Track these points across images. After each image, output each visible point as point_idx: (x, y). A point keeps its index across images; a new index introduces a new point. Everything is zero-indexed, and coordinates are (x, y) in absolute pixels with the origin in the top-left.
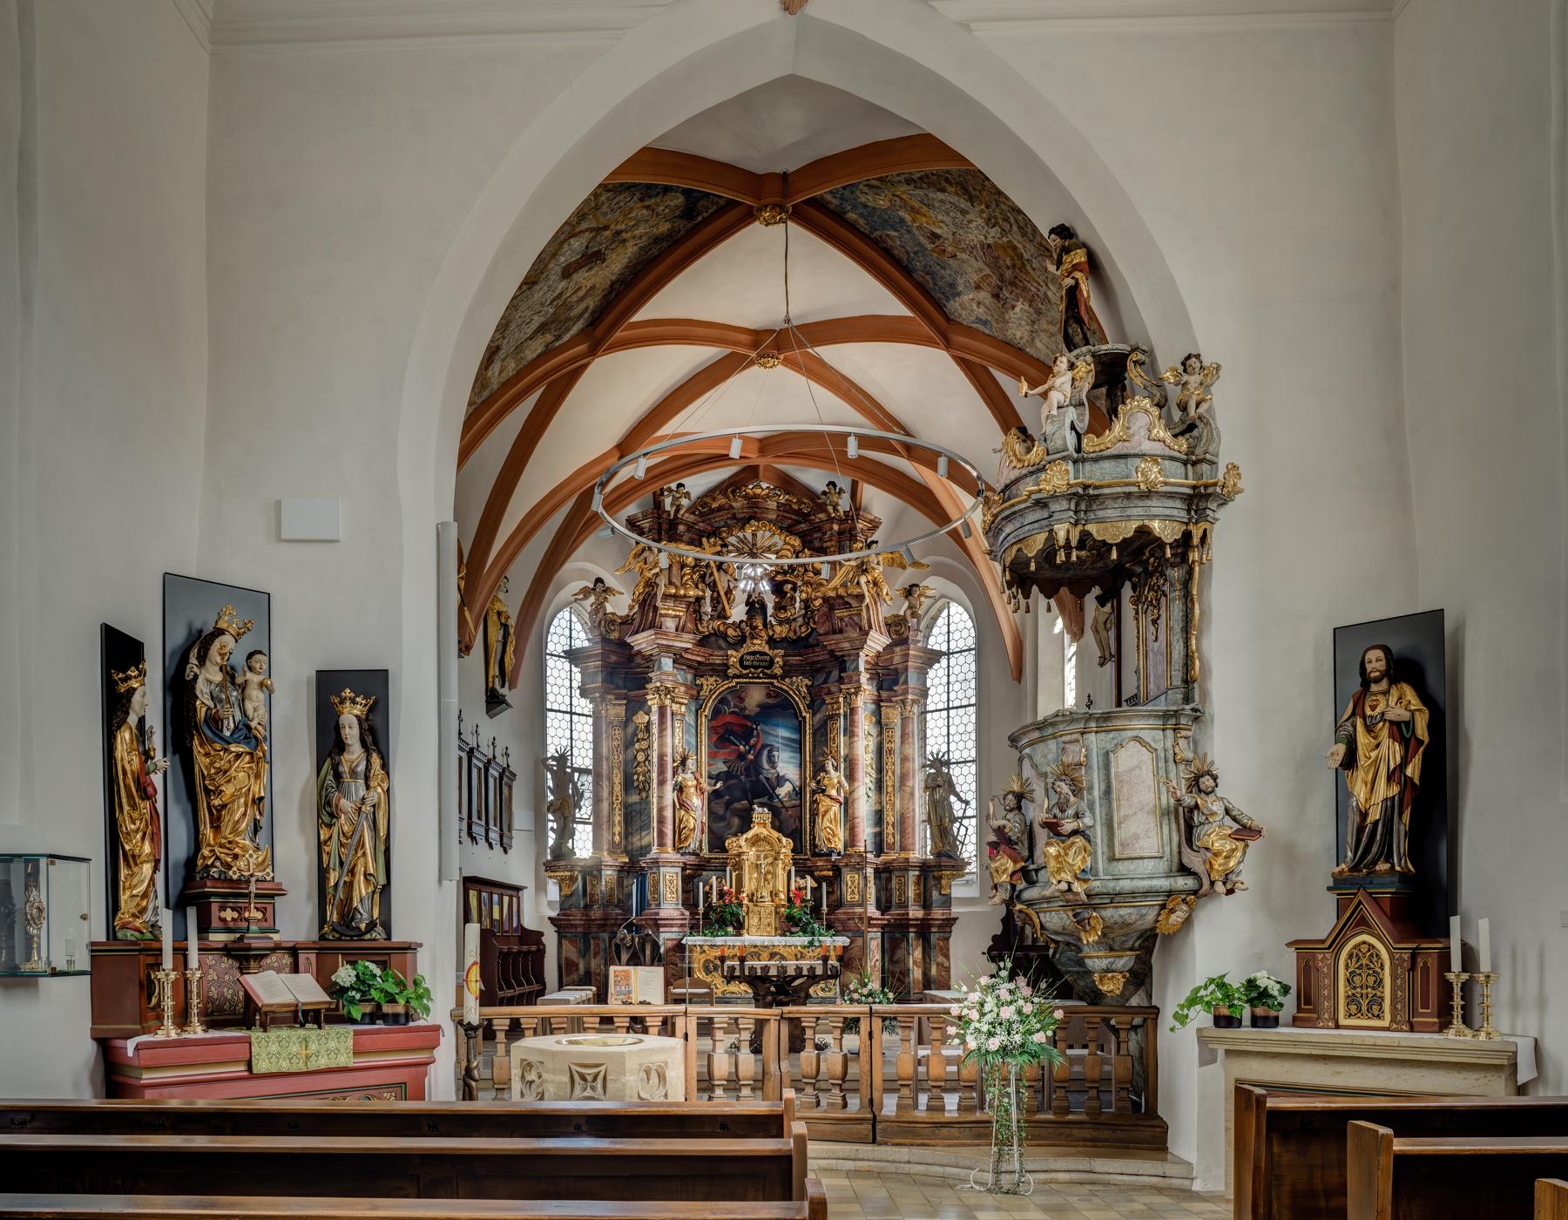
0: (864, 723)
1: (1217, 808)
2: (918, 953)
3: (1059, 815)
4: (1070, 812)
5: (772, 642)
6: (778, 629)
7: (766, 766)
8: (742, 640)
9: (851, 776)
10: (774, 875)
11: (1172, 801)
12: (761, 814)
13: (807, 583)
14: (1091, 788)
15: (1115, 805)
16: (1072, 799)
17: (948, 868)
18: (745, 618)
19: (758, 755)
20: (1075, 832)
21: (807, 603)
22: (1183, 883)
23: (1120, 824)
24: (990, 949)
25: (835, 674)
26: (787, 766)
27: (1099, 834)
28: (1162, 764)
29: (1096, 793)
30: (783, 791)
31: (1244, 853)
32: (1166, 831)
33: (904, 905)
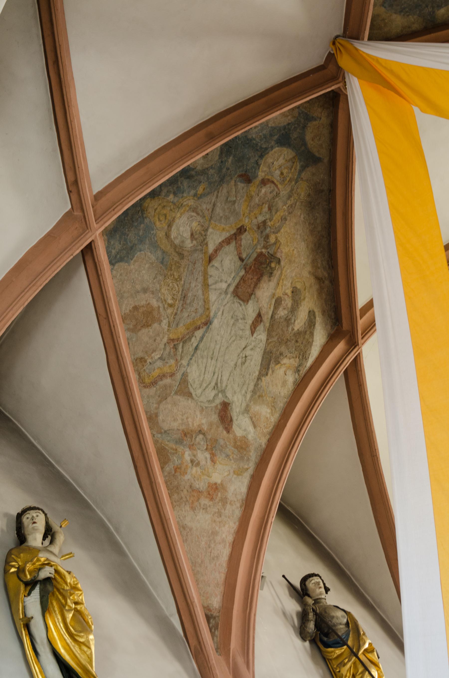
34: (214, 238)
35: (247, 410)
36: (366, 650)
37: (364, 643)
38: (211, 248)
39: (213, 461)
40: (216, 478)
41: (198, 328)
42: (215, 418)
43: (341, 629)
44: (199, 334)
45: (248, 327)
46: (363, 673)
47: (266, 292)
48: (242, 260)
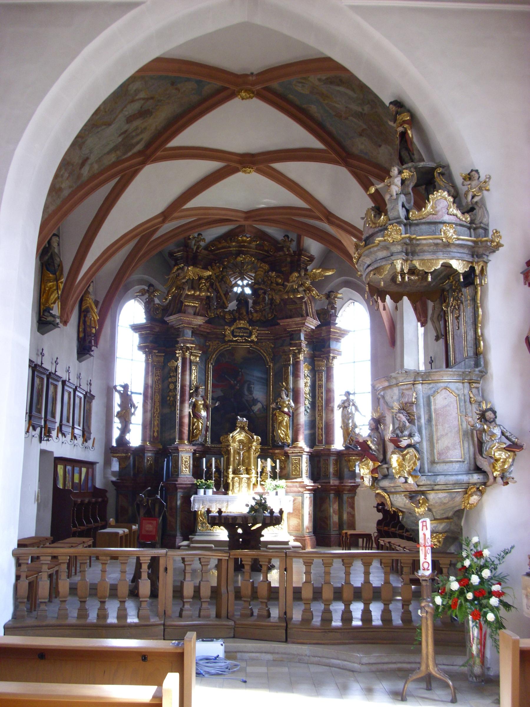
0: (304, 370)
1: (497, 431)
2: (336, 506)
3: (400, 434)
4: (406, 433)
5: (251, 322)
6: (255, 315)
9: (296, 400)
10: (249, 458)
11: (469, 427)
13: (272, 289)
14: (419, 418)
15: (434, 429)
16: (408, 424)
18: (236, 308)
20: (409, 446)
21: (272, 300)
22: (476, 478)
23: (438, 440)
26: (258, 393)
27: (425, 446)
28: (462, 404)
29: (423, 421)
30: (257, 408)
31: (513, 460)
32: (466, 445)
33: (327, 476)
34: (142, 95)
35: (92, 164)
38: (137, 97)
39: (67, 179)
40: (63, 186)
41: (105, 125)
42: (80, 161)
44: (103, 127)
45: (120, 133)
46: (55, 290)
47: (137, 123)
48: (141, 108)
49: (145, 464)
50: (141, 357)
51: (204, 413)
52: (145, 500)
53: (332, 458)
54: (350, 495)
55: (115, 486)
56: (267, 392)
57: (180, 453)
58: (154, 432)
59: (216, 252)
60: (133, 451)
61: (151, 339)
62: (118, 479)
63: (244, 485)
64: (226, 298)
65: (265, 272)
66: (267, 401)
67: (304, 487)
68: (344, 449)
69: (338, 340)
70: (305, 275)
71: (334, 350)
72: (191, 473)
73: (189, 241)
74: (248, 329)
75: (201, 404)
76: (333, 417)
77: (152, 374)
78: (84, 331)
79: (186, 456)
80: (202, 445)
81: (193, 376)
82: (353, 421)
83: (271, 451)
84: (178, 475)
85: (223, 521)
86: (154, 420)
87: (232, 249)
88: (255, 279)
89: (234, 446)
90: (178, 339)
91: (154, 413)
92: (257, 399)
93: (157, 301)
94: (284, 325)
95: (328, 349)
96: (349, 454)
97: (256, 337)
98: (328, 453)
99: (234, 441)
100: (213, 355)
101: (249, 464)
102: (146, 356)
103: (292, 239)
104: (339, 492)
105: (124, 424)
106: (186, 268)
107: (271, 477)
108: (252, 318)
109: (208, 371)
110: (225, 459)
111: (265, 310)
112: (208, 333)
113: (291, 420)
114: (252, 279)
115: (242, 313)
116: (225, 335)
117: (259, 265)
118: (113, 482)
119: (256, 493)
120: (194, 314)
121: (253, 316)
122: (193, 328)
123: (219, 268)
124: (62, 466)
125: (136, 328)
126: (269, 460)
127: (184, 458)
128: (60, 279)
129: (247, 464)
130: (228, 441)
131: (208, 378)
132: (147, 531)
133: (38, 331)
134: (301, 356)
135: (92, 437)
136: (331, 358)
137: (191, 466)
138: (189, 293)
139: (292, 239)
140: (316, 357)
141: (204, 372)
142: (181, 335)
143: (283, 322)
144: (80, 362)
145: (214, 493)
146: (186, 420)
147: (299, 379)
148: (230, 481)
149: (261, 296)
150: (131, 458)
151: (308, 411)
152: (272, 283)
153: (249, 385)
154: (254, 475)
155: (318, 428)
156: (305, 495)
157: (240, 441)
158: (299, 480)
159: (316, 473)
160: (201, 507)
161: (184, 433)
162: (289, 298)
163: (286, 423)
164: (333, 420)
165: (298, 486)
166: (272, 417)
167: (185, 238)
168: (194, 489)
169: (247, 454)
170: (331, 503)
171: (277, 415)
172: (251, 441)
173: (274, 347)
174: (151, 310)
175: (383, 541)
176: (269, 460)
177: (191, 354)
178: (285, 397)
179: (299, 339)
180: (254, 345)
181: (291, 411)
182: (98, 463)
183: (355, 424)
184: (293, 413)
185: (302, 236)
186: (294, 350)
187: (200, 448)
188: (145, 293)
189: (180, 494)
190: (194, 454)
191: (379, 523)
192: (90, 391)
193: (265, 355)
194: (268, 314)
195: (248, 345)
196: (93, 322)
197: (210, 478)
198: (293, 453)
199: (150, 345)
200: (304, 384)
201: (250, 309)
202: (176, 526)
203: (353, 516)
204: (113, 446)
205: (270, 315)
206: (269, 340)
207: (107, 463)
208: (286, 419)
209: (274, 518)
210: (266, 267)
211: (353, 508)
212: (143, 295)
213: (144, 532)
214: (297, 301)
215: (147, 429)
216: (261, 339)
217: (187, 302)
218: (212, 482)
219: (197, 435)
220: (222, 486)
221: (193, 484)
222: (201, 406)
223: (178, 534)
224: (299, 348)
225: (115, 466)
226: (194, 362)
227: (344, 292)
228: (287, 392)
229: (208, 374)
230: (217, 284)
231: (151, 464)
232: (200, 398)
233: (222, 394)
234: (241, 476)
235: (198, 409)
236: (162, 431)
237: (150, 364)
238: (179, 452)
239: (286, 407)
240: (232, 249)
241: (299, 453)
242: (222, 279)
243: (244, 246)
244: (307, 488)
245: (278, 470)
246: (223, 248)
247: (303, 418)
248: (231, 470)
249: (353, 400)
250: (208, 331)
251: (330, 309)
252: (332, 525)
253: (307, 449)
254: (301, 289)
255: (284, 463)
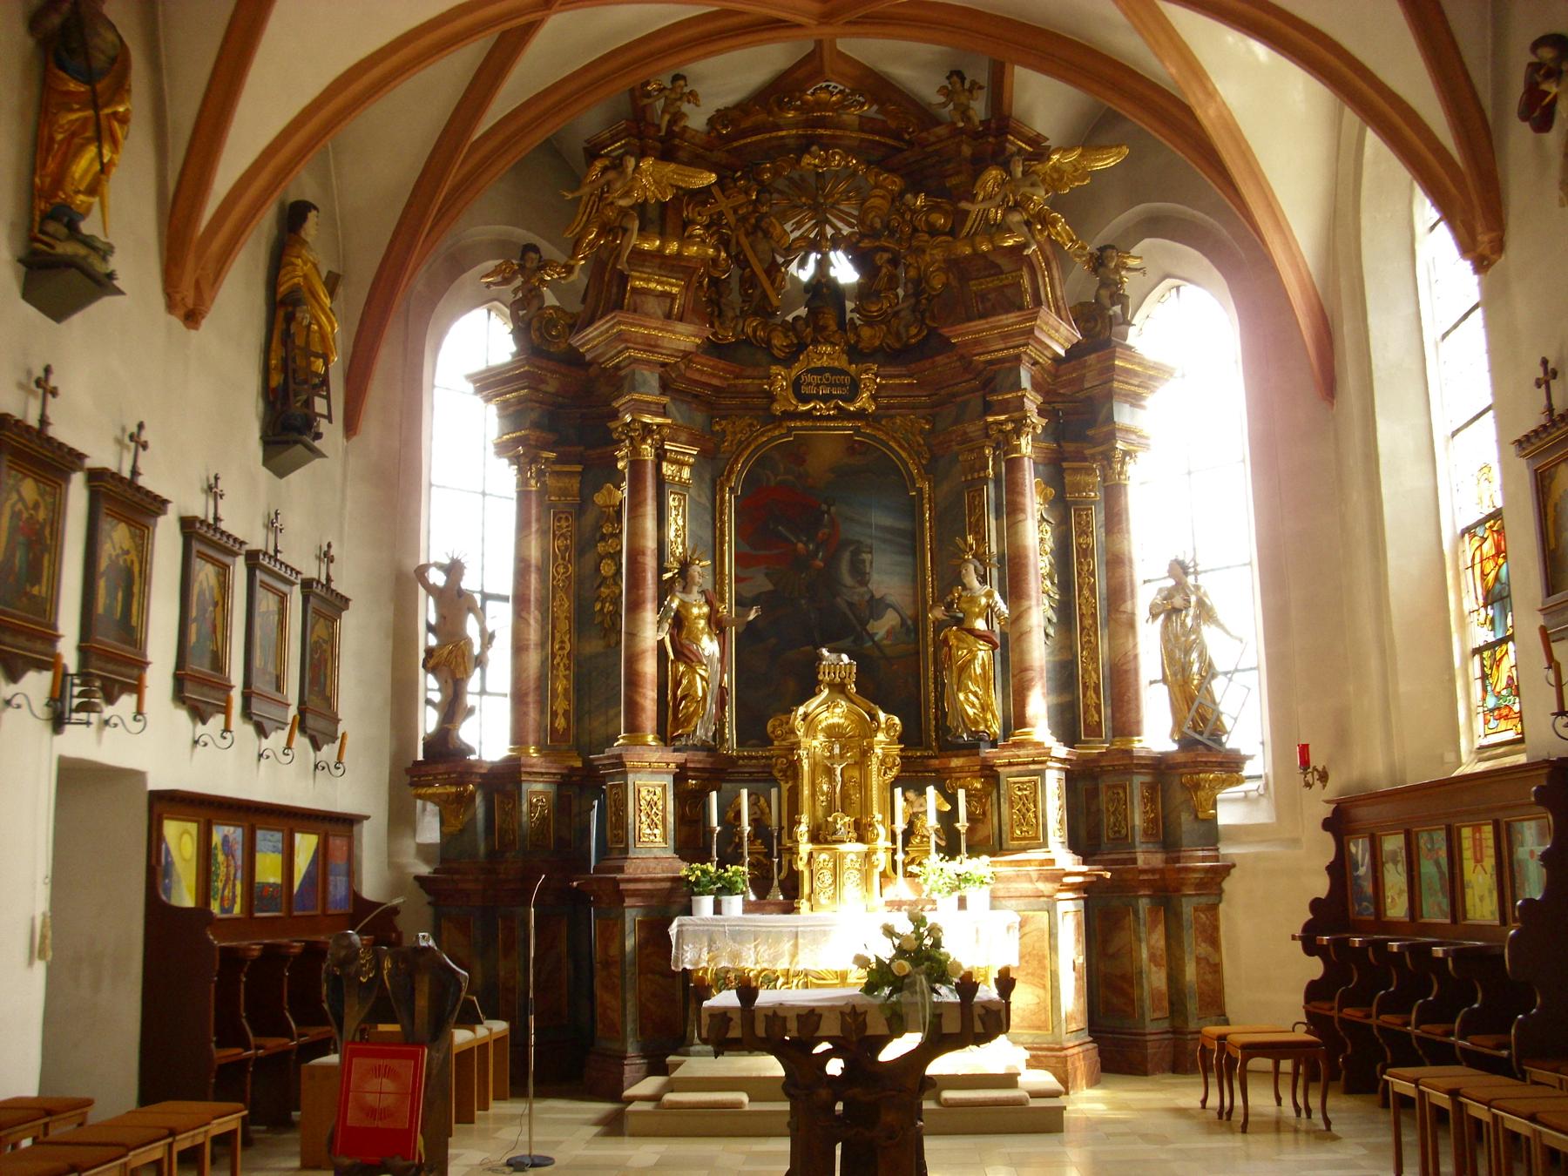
2: (1158, 939)
5: (855, 353)
6: (866, 332)
7: (848, 579)
8: (800, 347)
9: (1014, 589)
10: (864, 786)
12: (837, 662)
17: (1208, 766)
19: (832, 560)
24: (1308, 927)
25: (976, 403)
26: (887, 580)
30: (883, 626)
33: (1123, 840)
36: (115, 114)
37: (121, 102)
43: (100, 61)
49: (525, 819)
50: (505, 477)
51: (709, 646)
52: (365, 958)
53: (1139, 781)
54: (1203, 900)
55: (428, 892)
56: (915, 576)
57: (631, 777)
58: (554, 714)
59: (735, 144)
60: (482, 776)
61: (534, 416)
62: (435, 871)
63: (851, 879)
64: (773, 283)
65: (893, 201)
66: (915, 602)
67: (1057, 877)
68: (1174, 747)
69: (1135, 400)
70: (1024, 173)
71: (1128, 431)
72: (671, 843)
73: (646, 101)
74: (846, 373)
75: (699, 617)
76: (1135, 646)
77: (543, 533)
78: (285, 366)
79: (650, 789)
80: (704, 747)
81: (673, 527)
82: (1202, 654)
83: (935, 762)
84: (626, 850)
85: (760, 1031)
86: (555, 678)
87: (784, 133)
88: (861, 222)
89: (812, 746)
90: (616, 405)
91: (554, 656)
92: (882, 599)
93: (550, 299)
94: (965, 344)
95: (1105, 429)
96: (1195, 763)
97: (873, 397)
98: (1127, 763)
99: (811, 730)
100: (736, 461)
101: (866, 807)
102: (521, 471)
103: (973, 83)
104: (1166, 893)
105: (450, 691)
106: (631, 162)
107: (939, 849)
108: (857, 342)
109: (722, 513)
110: (785, 794)
111: (896, 314)
112: (716, 389)
113: (998, 658)
114: (850, 225)
115: (825, 328)
116: (771, 397)
117: (872, 181)
118: (418, 878)
119: (890, 904)
120: (668, 316)
121: (859, 336)
122: (664, 365)
123: (747, 193)
124: (192, 827)
125: (489, 383)
126: (931, 791)
127: (644, 793)
128: (107, 105)
129: (857, 806)
130: (792, 732)
131: (722, 534)
132: (372, 1112)
133: (28, 294)
134: (1023, 441)
135: (341, 729)
136: (1118, 455)
137: (671, 819)
138: (646, 246)
139: (973, 83)
140: (1065, 460)
141: (708, 518)
142: (626, 385)
143: (960, 334)
144: (281, 472)
145: (749, 908)
146: (649, 667)
147: (1021, 517)
148: (801, 865)
149: (884, 270)
150: (479, 800)
151: (1051, 631)
152: (915, 230)
153: (856, 554)
154: (882, 843)
155: (1085, 687)
156: (1062, 907)
157: (833, 732)
158: (1037, 855)
159: (1083, 833)
160: (705, 956)
161: (643, 709)
162: (977, 254)
163: (983, 666)
164: (1136, 656)
165: (1034, 875)
166: (935, 652)
167: (632, 90)
168: (678, 897)
169: (856, 774)
170: (1142, 929)
171: (953, 641)
172: (868, 729)
173: (932, 431)
174: (533, 327)
175: (1416, 1082)
176: (931, 791)
177: (661, 456)
178: (976, 584)
179: (1017, 385)
180: (868, 425)
181: (997, 628)
182: (367, 818)
183: (1210, 665)
184: (1004, 635)
185: (1008, 65)
186: (1001, 423)
187: (698, 759)
188: (515, 273)
189: (632, 915)
190: (680, 777)
191: (1314, 992)
192: (329, 579)
193: (904, 455)
194: (907, 326)
195: (845, 429)
196: (316, 338)
197: (737, 860)
198: (1010, 764)
199: (534, 435)
200: (1036, 536)
201: (849, 316)
202: (624, 1023)
203: (1216, 969)
204: (417, 763)
205: (913, 331)
206: (914, 408)
207: (401, 819)
208: (980, 654)
209: (978, 1011)
210: (894, 183)
211: (1214, 942)
212: (506, 281)
213: (354, 1118)
214: (1002, 262)
215: (527, 704)
216: (889, 407)
217: (640, 279)
218: (740, 871)
219: (688, 719)
220: (776, 882)
221: (677, 880)
222: (702, 623)
223: (631, 1050)
224: (1016, 415)
225: (430, 830)
226: (673, 484)
227: (1147, 249)
228: (981, 568)
229: (723, 523)
230: (744, 241)
231: (543, 819)
232: (695, 596)
233: (770, 587)
234: (841, 847)
235: (690, 632)
236: (579, 713)
237: (534, 498)
238: (625, 774)
239: (979, 615)
240: (784, 133)
241: (1034, 762)
242: (757, 227)
243: (822, 123)
244: (1067, 880)
245: (962, 825)
246: (756, 130)
247: (1039, 651)
248: (803, 829)
249: (1197, 588)
250: (715, 382)
251: (1107, 302)
252: (1147, 1003)
253: (1061, 751)
254: (1016, 218)
255: (980, 799)
